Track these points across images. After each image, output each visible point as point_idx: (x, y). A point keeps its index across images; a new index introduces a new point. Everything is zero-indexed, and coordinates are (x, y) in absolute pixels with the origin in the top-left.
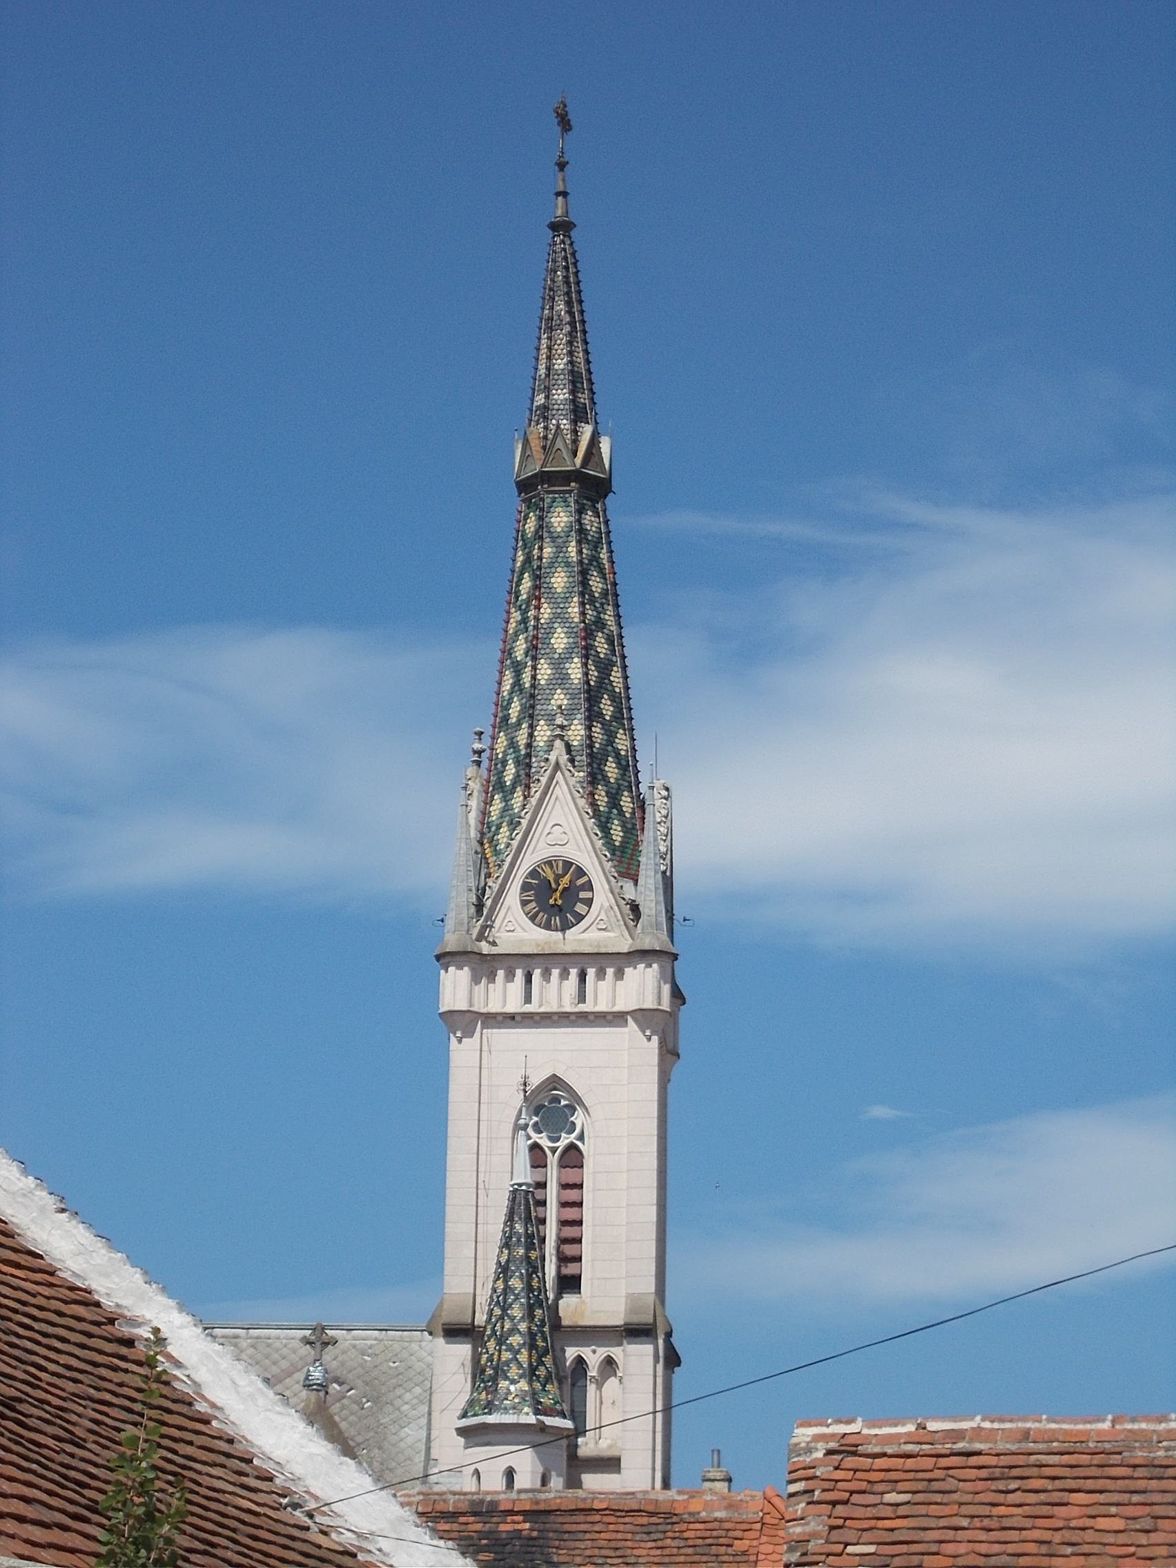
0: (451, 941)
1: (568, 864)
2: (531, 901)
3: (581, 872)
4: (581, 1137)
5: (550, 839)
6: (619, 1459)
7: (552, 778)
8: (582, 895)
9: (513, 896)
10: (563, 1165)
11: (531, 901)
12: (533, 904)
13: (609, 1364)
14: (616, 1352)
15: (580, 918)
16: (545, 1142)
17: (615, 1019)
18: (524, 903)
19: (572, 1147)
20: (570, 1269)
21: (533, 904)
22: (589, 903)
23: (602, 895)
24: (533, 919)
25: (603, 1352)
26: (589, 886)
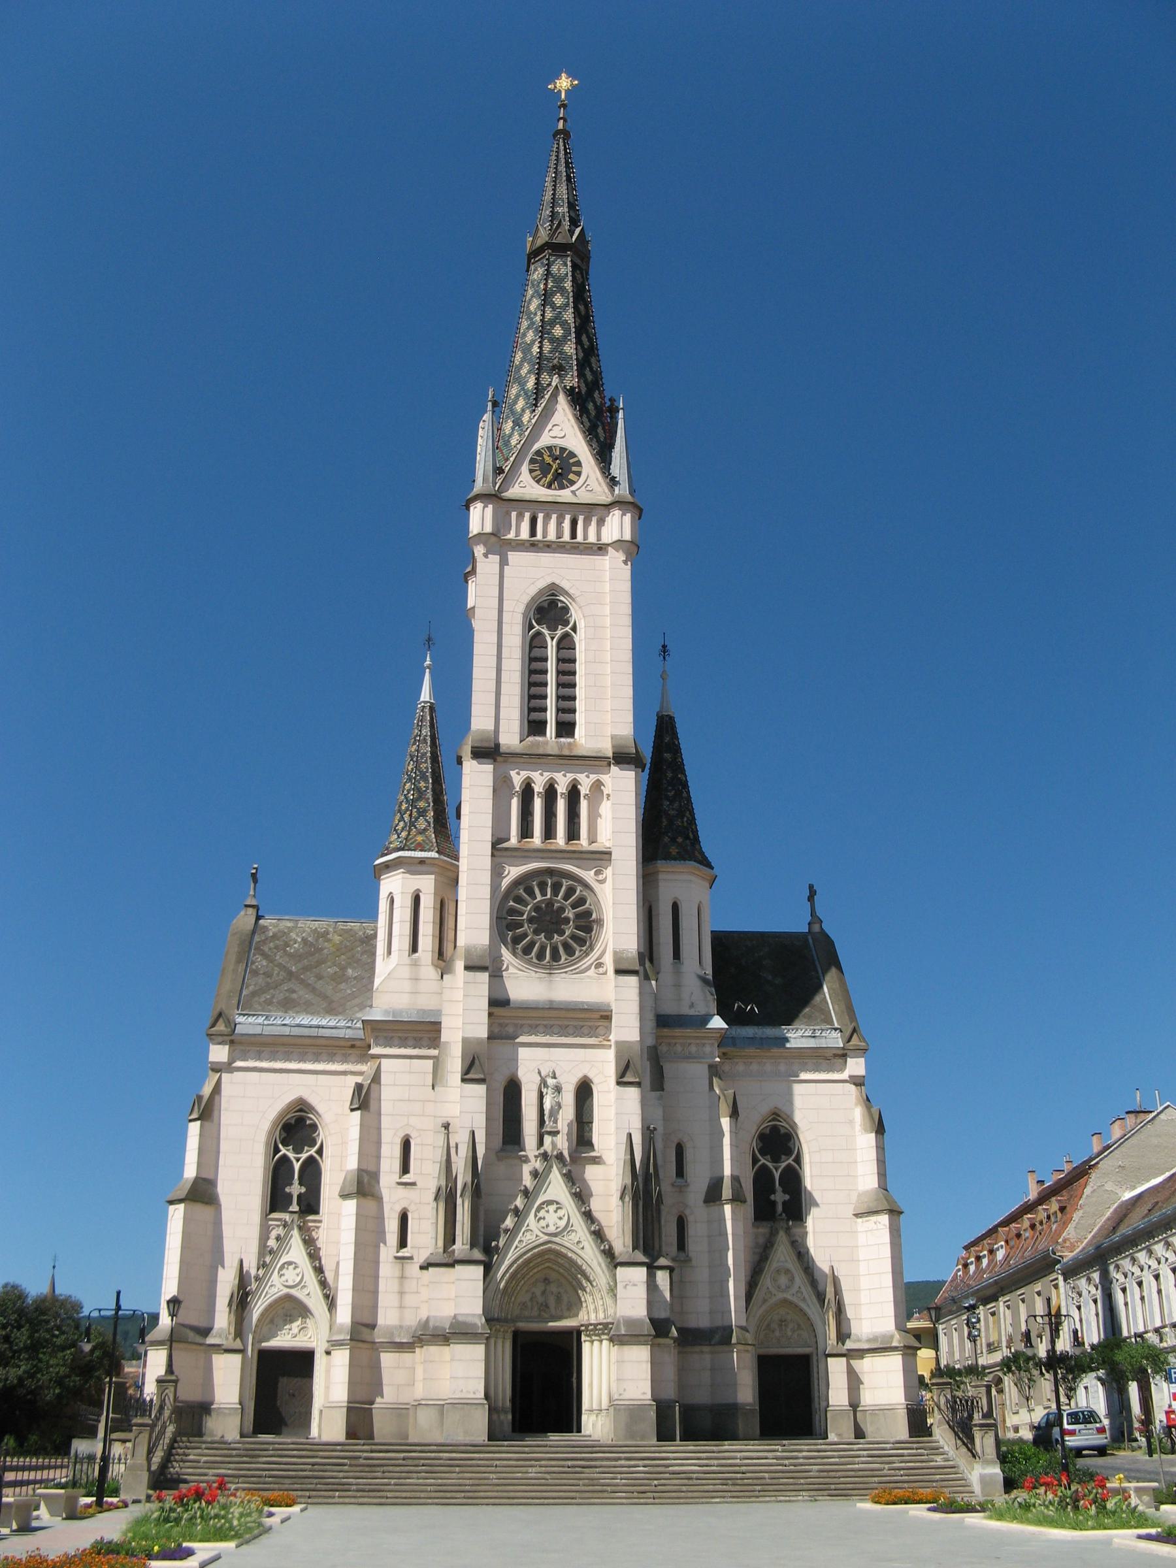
0: (479, 486)
1: (563, 450)
2: (536, 470)
3: (572, 455)
4: (574, 629)
5: (552, 434)
6: (610, 853)
7: (554, 396)
8: (574, 469)
9: (525, 468)
10: (559, 647)
11: (536, 470)
12: (538, 472)
13: (598, 786)
14: (605, 778)
15: (572, 483)
16: (546, 632)
18: (531, 471)
19: (566, 636)
20: (566, 717)
21: (538, 472)
22: (579, 474)
24: (538, 482)
25: (593, 777)
26: (579, 464)
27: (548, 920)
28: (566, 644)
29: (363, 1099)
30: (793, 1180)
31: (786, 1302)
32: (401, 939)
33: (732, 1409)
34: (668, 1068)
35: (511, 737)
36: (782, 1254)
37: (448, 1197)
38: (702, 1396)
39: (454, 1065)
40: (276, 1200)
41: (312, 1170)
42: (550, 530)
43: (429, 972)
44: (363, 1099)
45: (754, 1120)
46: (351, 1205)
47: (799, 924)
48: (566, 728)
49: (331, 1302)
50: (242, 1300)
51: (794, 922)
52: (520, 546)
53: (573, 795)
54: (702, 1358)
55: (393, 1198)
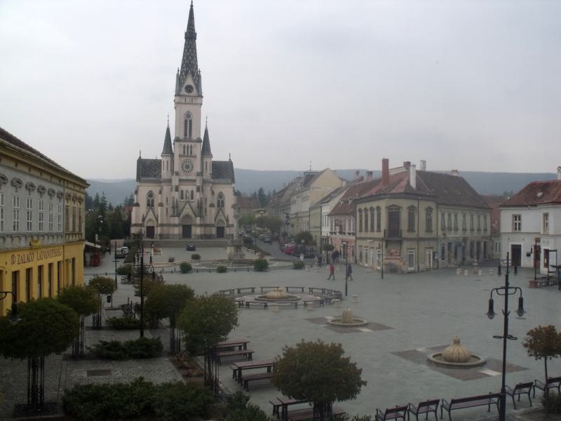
17: (196, 104)
23: (195, 90)
27: (187, 167)
28: (191, 121)
29: (160, 192)
30: (223, 202)
31: (220, 220)
32: (165, 168)
33: (212, 235)
34: (204, 188)
35: (182, 137)
36: (221, 213)
37: (173, 207)
38: (208, 233)
39: (174, 189)
40: (148, 205)
41: (153, 201)
42: (188, 100)
43: (170, 174)
44: (160, 192)
45: (217, 192)
46: (160, 208)
47: (227, 160)
48: (190, 135)
49: (157, 220)
50: (144, 220)
51: (227, 159)
52: (182, 103)
53: (191, 147)
54: (208, 228)
55: (165, 206)
